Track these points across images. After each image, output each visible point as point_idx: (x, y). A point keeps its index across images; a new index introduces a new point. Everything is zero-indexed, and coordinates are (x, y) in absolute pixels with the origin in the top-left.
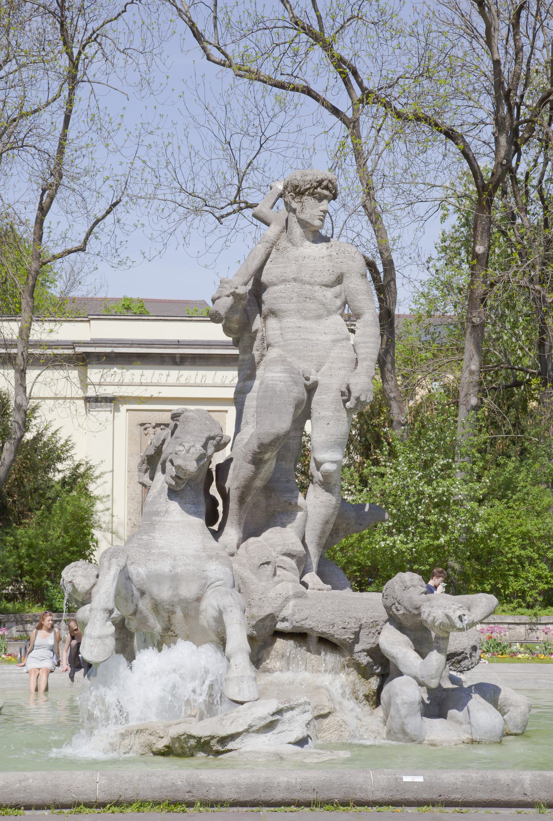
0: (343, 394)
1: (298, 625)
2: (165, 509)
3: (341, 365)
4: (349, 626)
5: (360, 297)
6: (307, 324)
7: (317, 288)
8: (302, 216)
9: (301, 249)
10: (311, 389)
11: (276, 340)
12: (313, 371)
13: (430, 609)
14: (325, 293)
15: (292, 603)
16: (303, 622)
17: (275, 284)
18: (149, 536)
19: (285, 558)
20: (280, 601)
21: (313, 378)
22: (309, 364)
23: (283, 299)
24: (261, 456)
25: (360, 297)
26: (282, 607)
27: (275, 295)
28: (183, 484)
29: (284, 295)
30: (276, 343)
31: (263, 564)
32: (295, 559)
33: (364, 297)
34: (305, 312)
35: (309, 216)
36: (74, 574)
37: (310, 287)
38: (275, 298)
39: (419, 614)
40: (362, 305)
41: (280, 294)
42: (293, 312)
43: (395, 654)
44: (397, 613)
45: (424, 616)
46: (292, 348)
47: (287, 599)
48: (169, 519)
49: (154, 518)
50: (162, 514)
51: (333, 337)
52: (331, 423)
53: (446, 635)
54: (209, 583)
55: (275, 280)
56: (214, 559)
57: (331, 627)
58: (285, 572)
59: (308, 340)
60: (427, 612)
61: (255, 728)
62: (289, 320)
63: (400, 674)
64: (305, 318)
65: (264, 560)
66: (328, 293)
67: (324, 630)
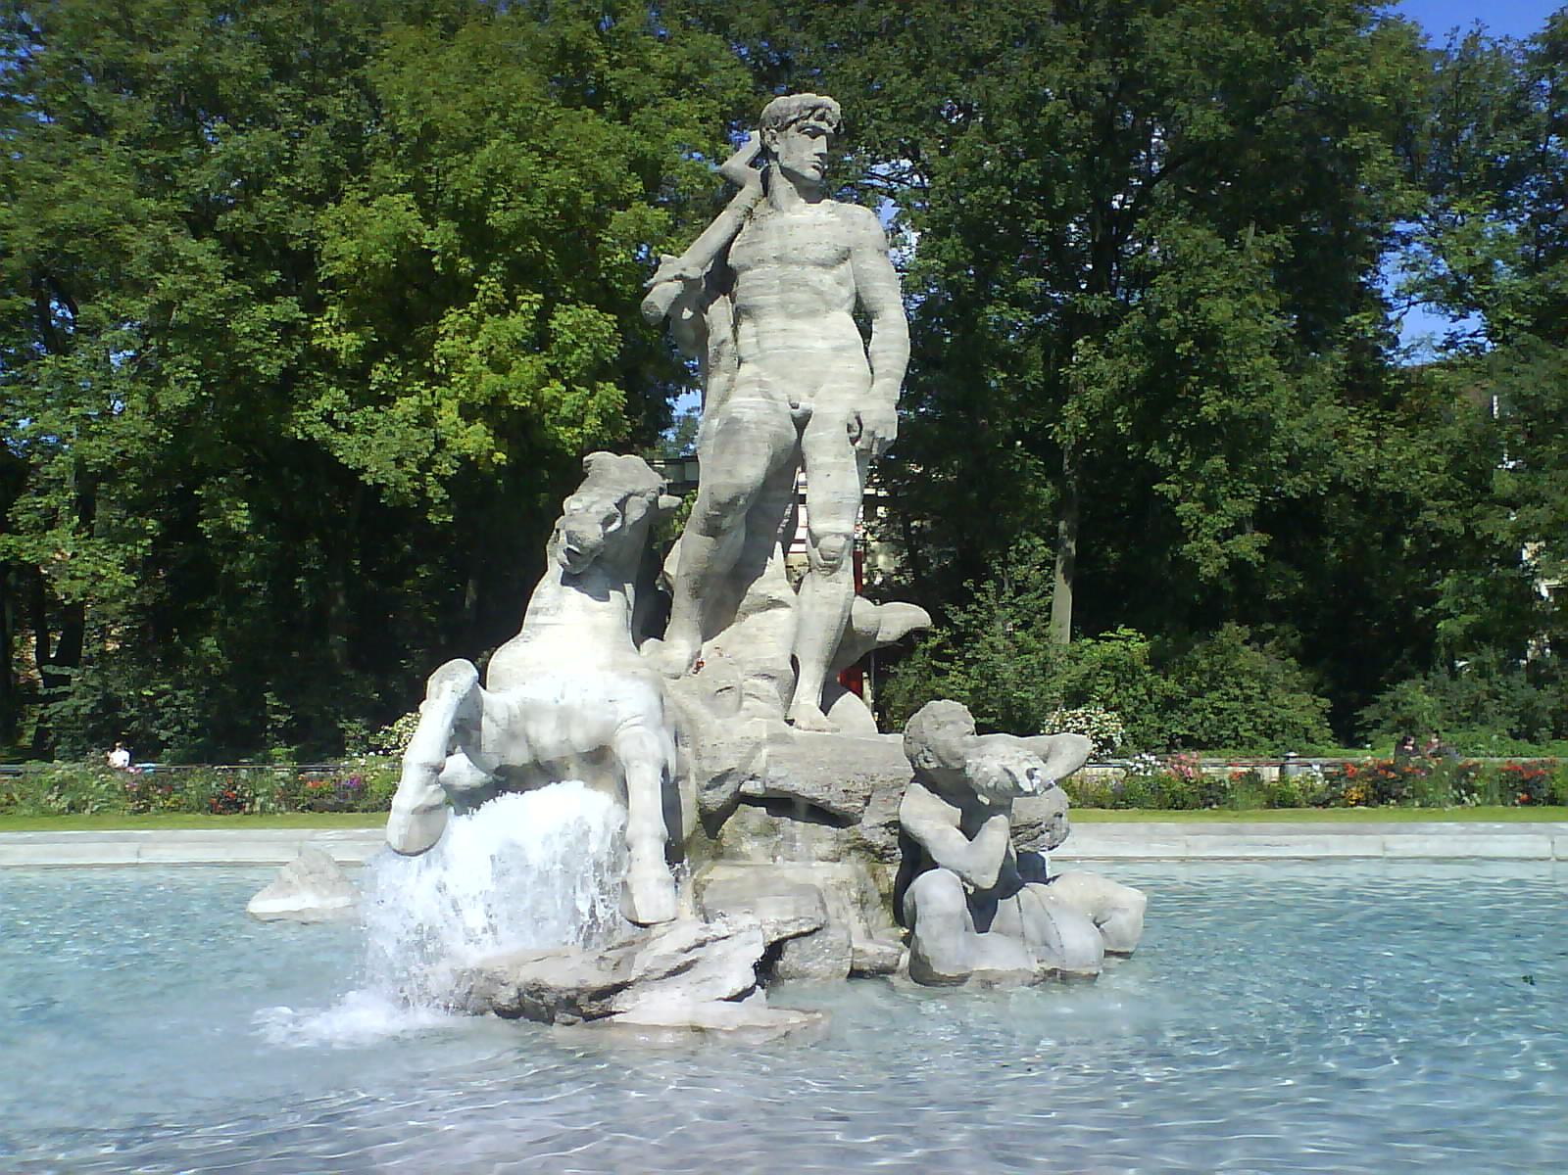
0: (849, 428)
1: (773, 786)
3: (847, 385)
5: (876, 284)
8: (786, 164)
9: (787, 215)
10: (801, 423)
12: (805, 396)
13: (979, 760)
14: (822, 276)
15: (765, 751)
16: (780, 783)
17: (749, 269)
19: (759, 682)
20: (747, 749)
21: (804, 405)
24: (718, 523)
25: (876, 284)
26: (751, 757)
28: (585, 563)
30: (750, 356)
31: (721, 691)
32: (775, 682)
33: (883, 284)
39: (963, 769)
43: (923, 835)
44: (926, 765)
45: (970, 772)
47: (758, 746)
50: (552, 612)
51: (837, 343)
52: (833, 474)
53: (1007, 803)
54: (619, 720)
55: (747, 262)
58: (758, 702)
60: (974, 765)
61: (657, 975)
63: (935, 866)
64: (793, 316)
65: (723, 684)
66: (827, 277)
67: (815, 795)
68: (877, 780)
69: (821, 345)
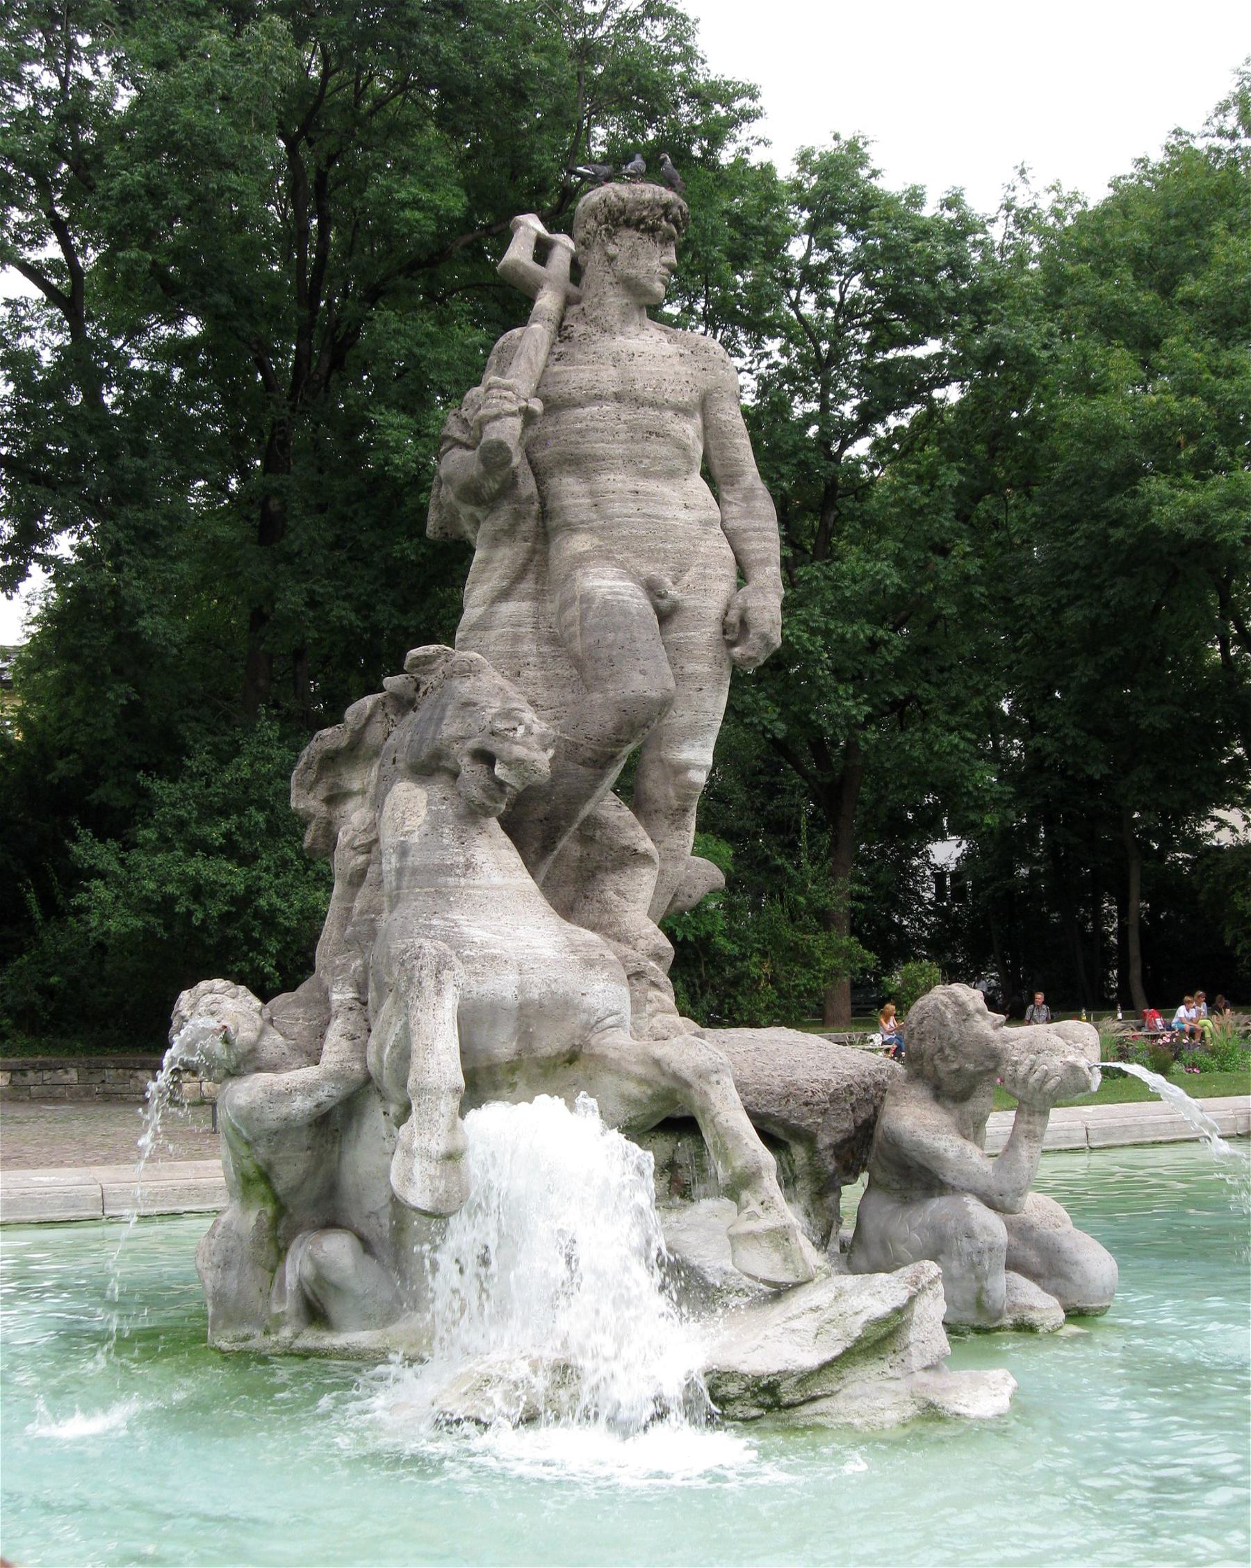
2: (462, 859)
3: (720, 572)
4: (816, 1099)
5: (737, 441)
6: (651, 486)
7: (669, 414)
9: (620, 338)
11: (583, 517)
13: (1033, 1057)
17: (580, 405)
18: (446, 919)
22: (658, 566)
23: (599, 434)
25: (737, 441)
27: (579, 426)
29: (601, 425)
34: (646, 461)
35: (643, 272)
36: (215, 1006)
37: (657, 413)
38: (580, 432)
40: (742, 457)
41: (591, 424)
42: (620, 461)
46: (625, 533)
48: (477, 882)
49: (441, 880)
54: (592, 1022)
55: (578, 395)
56: (598, 968)
57: (783, 1102)
59: (658, 517)
60: (1027, 1061)
62: (612, 477)
64: (646, 474)
67: (772, 1110)
68: (834, 1085)
69: (683, 515)
